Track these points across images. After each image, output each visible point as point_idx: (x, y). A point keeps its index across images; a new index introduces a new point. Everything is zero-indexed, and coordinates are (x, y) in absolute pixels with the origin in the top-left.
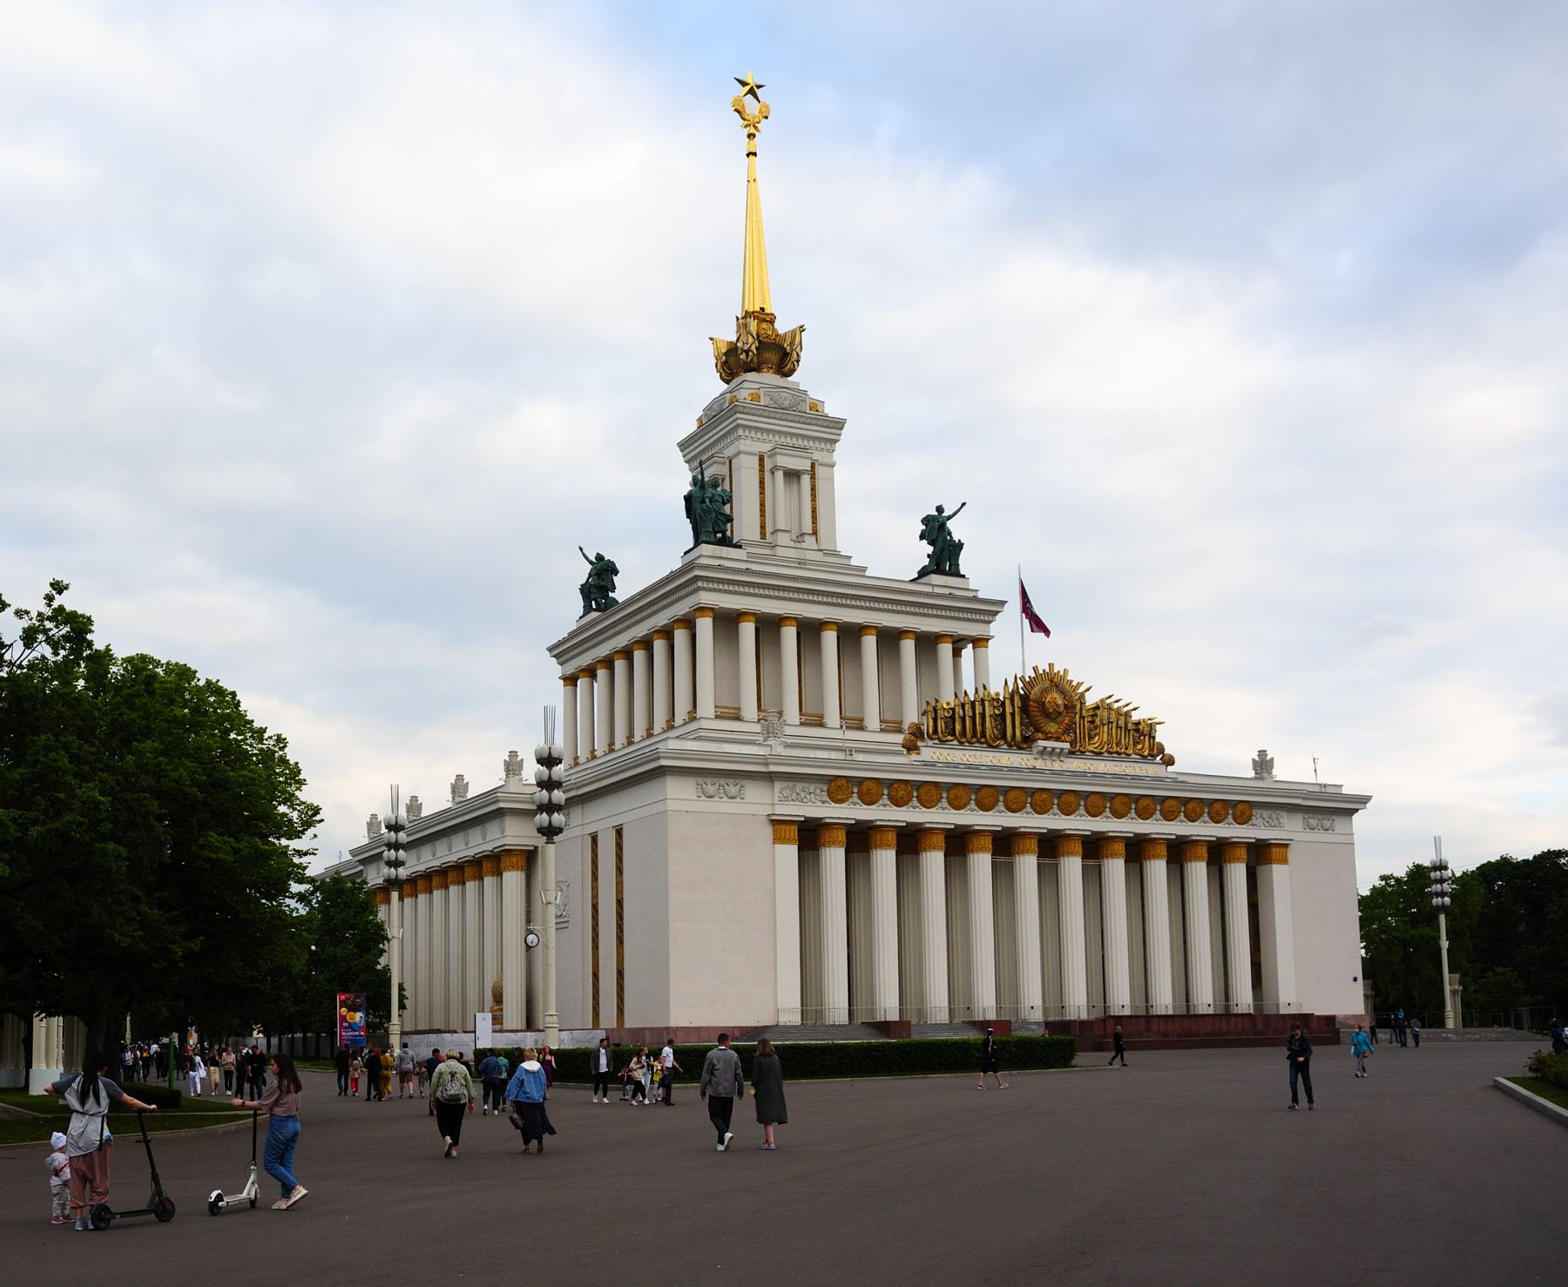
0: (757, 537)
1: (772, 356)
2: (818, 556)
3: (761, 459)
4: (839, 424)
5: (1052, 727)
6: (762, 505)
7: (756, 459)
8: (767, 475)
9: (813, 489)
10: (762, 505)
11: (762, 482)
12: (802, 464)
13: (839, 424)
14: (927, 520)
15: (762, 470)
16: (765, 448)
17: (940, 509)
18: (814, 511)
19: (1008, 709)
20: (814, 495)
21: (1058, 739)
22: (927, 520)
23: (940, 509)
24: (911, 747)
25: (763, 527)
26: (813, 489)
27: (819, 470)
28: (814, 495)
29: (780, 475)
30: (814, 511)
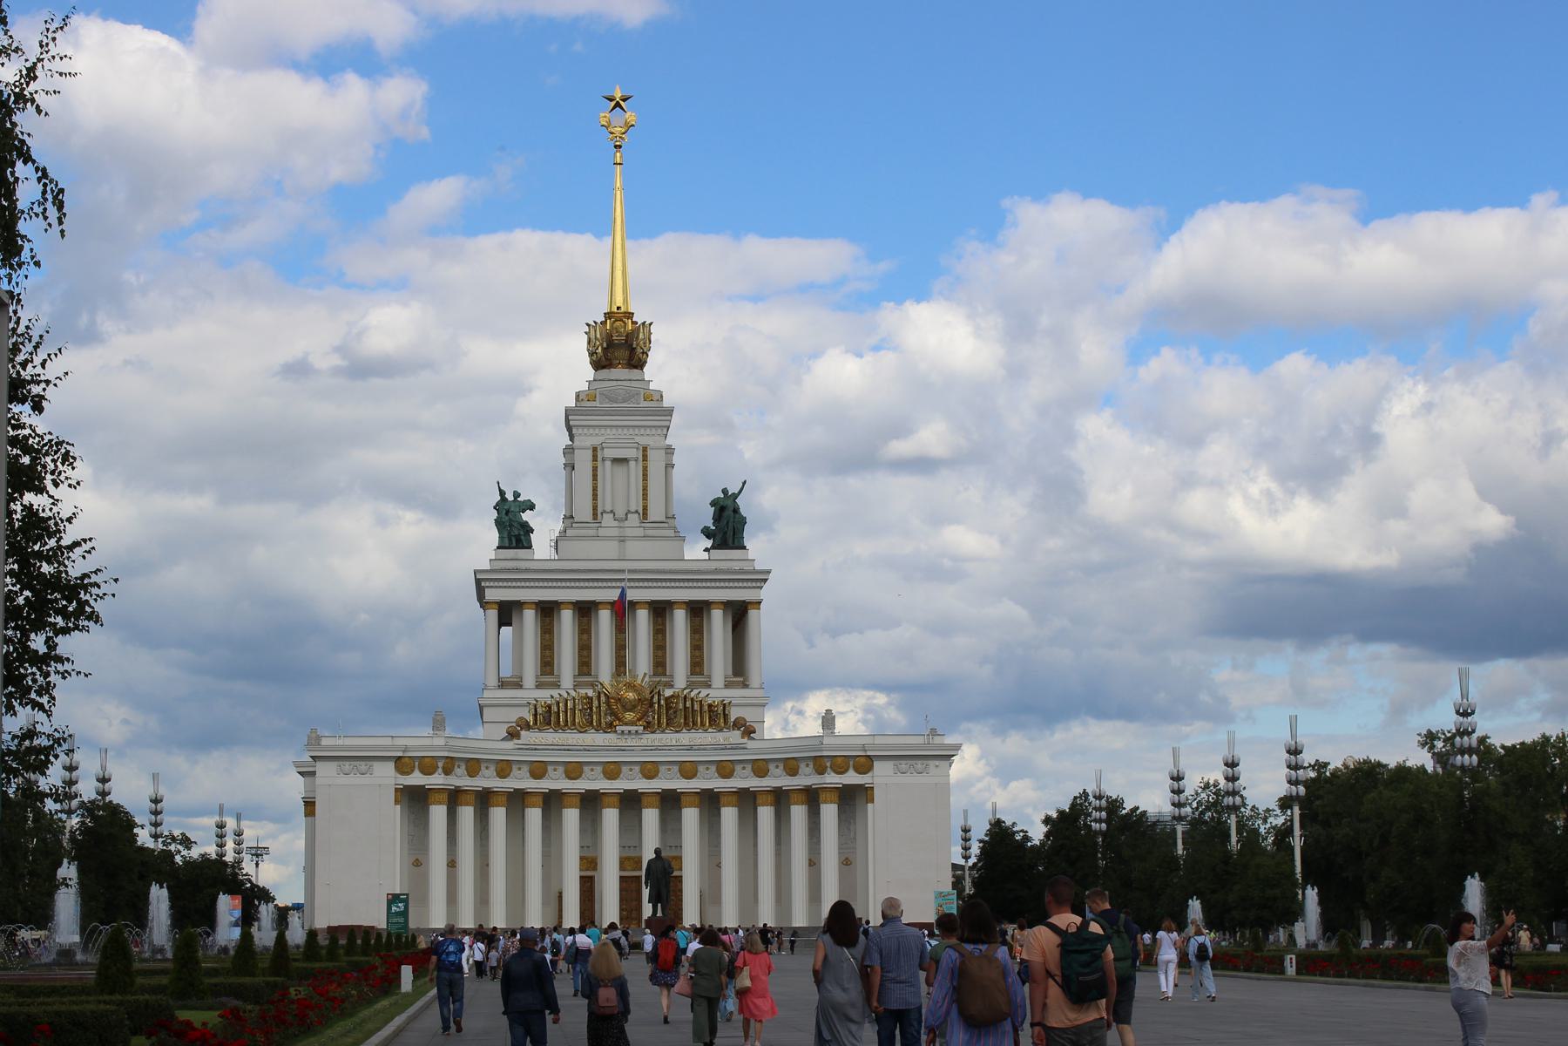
0: (590, 519)
1: (623, 354)
2: (640, 532)
3: (595, 450)
4: (669, 412)
5: (629, 716)
6: (595, 489)
7: (590, 452)
8: (599, 464)
9: (645, 469)
10: (595, 489)
11: (595, 469)
12: (630, 453)
13: (669, 412)
14: (713, 504)
15: (595, 458)
16: (596, 441)
17: (725, 491)
18: (645, 489)
19: (595, 703)
20: (645, 476)
21: (632, 723)
22: (713, 504)
23: (725, 491)
24: (512, 735)
25: (595, 508)
26: (645, 469)
27: (650, 452)
28: (645, 476)
29: (608, 463)
30: (645, 489)
